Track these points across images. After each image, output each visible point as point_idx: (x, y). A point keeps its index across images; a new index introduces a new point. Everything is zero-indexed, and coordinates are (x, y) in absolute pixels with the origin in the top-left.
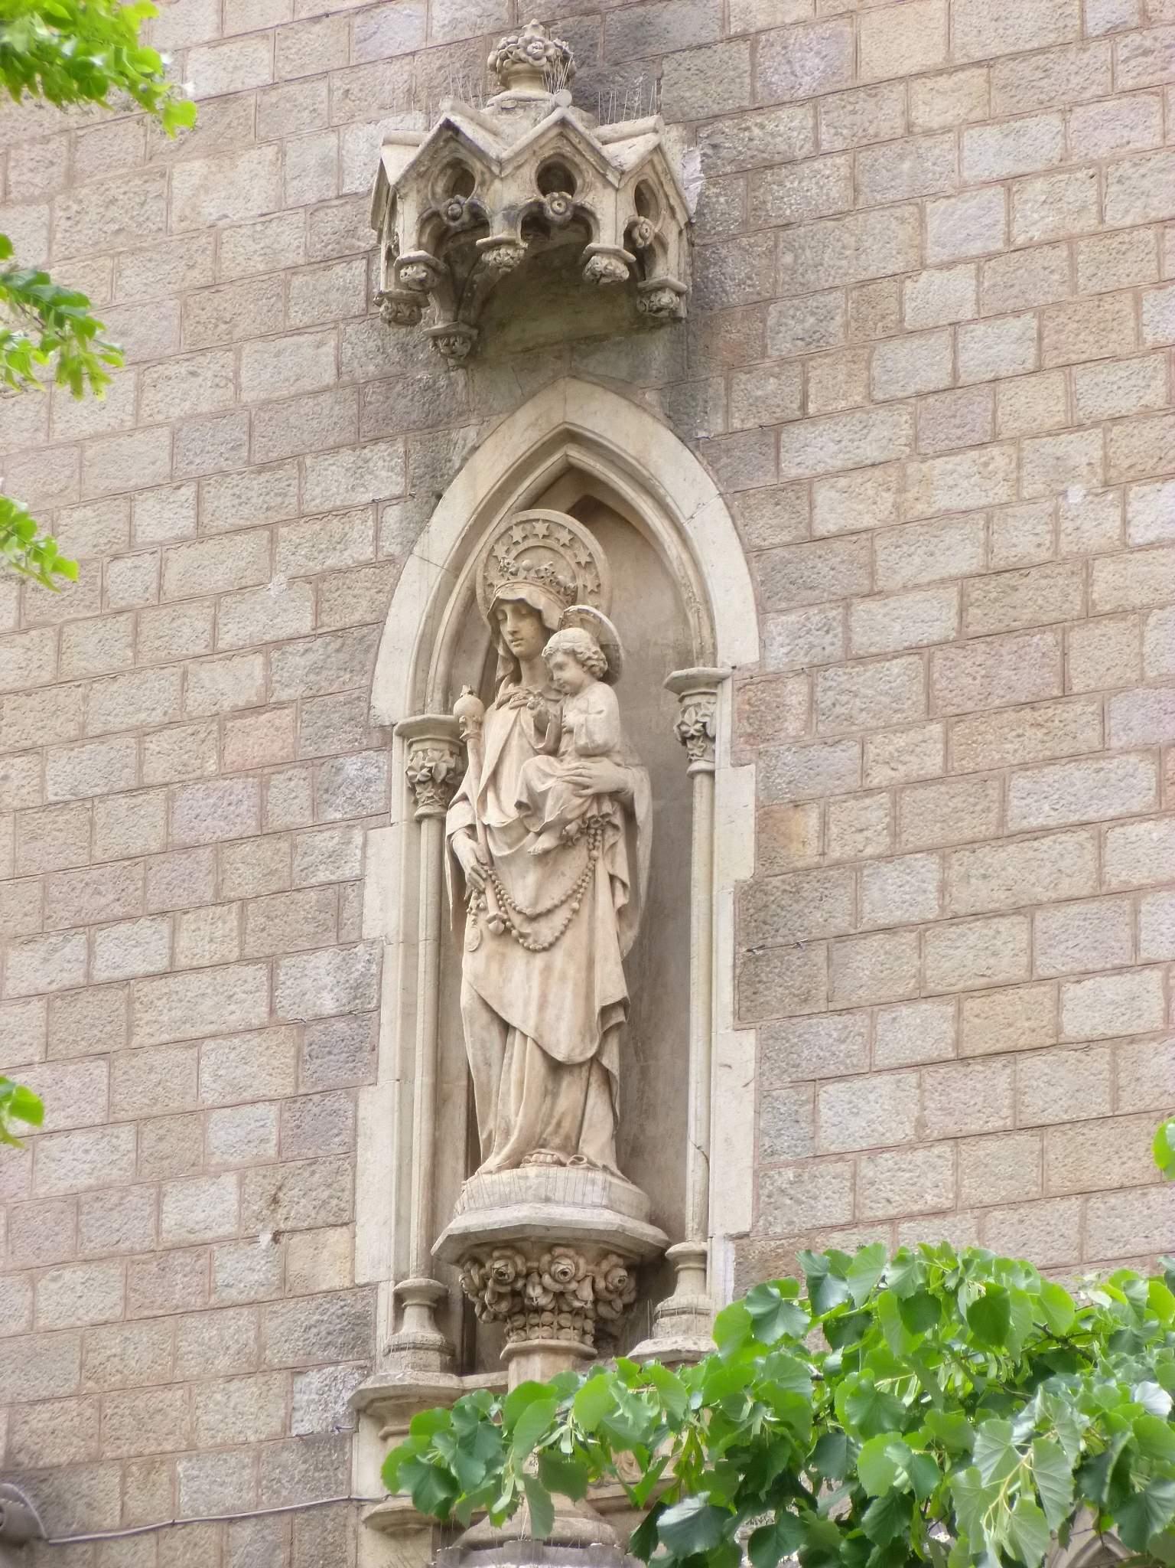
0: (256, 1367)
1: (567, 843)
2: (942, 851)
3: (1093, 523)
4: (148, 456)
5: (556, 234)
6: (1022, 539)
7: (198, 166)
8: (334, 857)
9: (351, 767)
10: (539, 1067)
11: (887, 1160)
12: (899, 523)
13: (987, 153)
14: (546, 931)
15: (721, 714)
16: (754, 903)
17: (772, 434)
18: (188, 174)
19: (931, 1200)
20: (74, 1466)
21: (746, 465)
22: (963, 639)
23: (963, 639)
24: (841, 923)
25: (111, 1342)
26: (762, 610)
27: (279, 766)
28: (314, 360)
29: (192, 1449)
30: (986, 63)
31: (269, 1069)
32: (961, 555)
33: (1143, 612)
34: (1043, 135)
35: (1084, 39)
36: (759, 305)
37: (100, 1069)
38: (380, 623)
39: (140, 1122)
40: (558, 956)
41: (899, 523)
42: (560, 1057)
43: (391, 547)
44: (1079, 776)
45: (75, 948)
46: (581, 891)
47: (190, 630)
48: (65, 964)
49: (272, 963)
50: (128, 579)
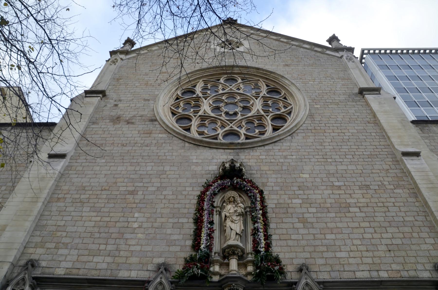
2: (276, 223)
4: (188, 184)
6: (281, 201)
7: (194, 167)
10: (235, 233)
14: (236, 222)
18: (193, 167)
20: (173, 264)
23: (276, 208)
25: (179, 253)
30: (273, 170)
32: (276, 202)
33: (295, 208)
35: (282, 170)
37: (179, 230)
39: (183, 235)
40: (238, 224)
42: (238, 232)
44: (290, 219)
46: (240, 219)
48: (176, 220)
50: (184, 193)
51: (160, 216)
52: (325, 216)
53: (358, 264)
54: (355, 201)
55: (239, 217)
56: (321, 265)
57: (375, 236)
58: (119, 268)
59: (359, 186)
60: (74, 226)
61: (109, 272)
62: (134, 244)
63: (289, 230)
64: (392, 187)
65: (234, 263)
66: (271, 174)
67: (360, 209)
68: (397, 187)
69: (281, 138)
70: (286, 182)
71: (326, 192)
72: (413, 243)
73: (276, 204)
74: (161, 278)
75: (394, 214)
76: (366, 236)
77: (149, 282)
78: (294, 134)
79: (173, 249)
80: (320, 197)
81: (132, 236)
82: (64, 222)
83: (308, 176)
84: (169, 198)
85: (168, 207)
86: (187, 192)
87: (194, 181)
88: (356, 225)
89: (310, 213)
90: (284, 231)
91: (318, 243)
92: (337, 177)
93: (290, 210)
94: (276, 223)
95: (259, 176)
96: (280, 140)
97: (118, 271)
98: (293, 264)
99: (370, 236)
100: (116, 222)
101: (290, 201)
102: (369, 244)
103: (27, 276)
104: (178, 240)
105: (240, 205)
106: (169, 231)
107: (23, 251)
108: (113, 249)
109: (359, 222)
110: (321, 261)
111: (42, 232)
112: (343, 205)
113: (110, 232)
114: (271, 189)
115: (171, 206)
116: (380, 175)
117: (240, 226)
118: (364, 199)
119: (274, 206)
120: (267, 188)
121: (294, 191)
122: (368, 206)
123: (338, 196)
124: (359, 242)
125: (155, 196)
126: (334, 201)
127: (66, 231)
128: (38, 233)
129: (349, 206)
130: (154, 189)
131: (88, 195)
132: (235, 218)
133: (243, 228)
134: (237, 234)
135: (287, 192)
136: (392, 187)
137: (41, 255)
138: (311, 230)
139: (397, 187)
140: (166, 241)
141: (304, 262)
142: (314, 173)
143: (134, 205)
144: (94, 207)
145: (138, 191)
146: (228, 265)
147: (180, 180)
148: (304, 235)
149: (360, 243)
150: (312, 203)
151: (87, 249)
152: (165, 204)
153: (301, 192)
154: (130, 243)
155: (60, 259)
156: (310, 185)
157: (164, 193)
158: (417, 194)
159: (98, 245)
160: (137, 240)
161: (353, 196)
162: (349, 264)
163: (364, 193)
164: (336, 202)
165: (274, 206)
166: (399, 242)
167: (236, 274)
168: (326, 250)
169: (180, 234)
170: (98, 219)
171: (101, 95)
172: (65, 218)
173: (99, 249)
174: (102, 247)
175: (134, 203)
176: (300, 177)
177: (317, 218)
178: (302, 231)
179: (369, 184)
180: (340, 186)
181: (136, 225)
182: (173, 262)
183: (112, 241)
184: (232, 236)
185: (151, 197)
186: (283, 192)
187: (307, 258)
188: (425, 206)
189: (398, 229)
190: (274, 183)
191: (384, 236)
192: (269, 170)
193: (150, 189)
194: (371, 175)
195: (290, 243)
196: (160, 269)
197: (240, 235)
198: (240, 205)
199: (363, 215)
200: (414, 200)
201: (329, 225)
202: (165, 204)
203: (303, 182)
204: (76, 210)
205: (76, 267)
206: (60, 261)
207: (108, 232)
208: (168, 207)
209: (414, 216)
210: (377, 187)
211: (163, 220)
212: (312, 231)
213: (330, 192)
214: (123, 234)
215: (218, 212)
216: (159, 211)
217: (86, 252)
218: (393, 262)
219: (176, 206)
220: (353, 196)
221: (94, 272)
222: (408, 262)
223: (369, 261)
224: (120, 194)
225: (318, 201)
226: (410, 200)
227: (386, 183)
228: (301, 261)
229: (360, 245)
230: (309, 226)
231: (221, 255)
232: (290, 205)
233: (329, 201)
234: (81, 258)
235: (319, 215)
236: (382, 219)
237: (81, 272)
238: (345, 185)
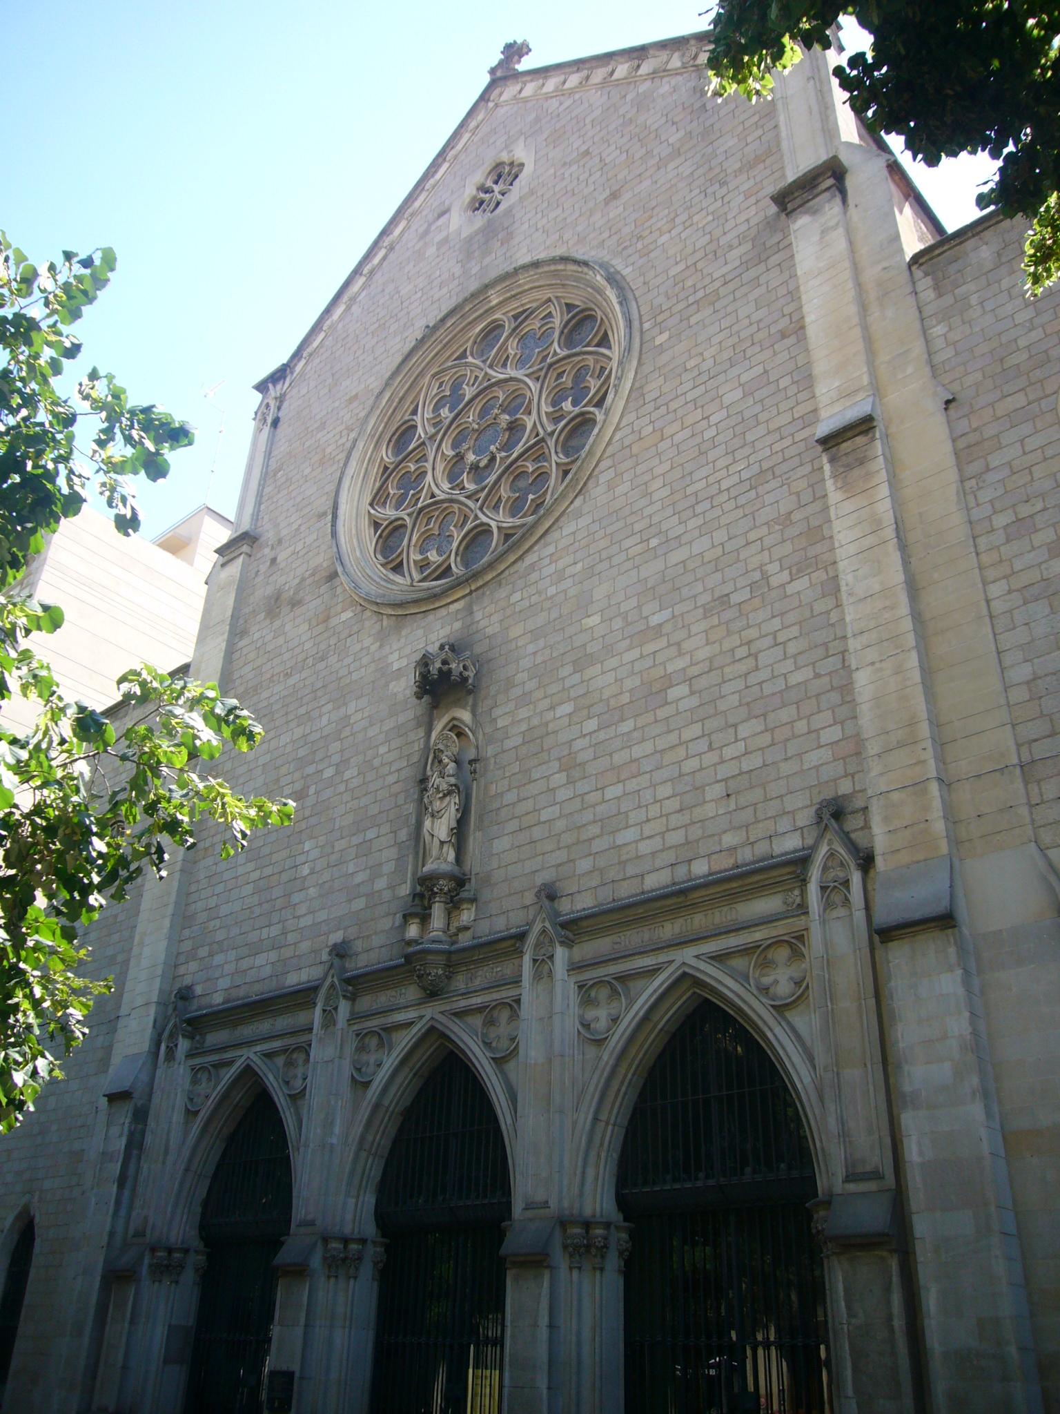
1: (445, 796)
2: (518, 787)
3: (549, 716)
5: (445, 675)
13: (531, 648)
22: (523, 744)
28: (410, 714)
29: (376, 933)
32: (524, 727)
34: (541, 643)
36: (488, 687)
41: (513, 723)
44: (544, 767)
68: (799, 571)
69: (557, 514)
77: (315, 989)
78: (591, 484)
88: (673, 738)
91: (588, 816)
96: (557, 520)
99: (692, 764)
110: (584, 865)
128: (186, 933)
139: (799, 571)
161: (686, 646)
163: (712, 627)
164: (642, 684)
166: (755, 761)
171: (245, 548)
180: (660, 625)
187: (560, 865)
195: (537, 833)
199: (694, 701)
212: (582, 787)
213: (635, 653)
227: (773, 568)
229: (668, 798)
235: (602, 735)
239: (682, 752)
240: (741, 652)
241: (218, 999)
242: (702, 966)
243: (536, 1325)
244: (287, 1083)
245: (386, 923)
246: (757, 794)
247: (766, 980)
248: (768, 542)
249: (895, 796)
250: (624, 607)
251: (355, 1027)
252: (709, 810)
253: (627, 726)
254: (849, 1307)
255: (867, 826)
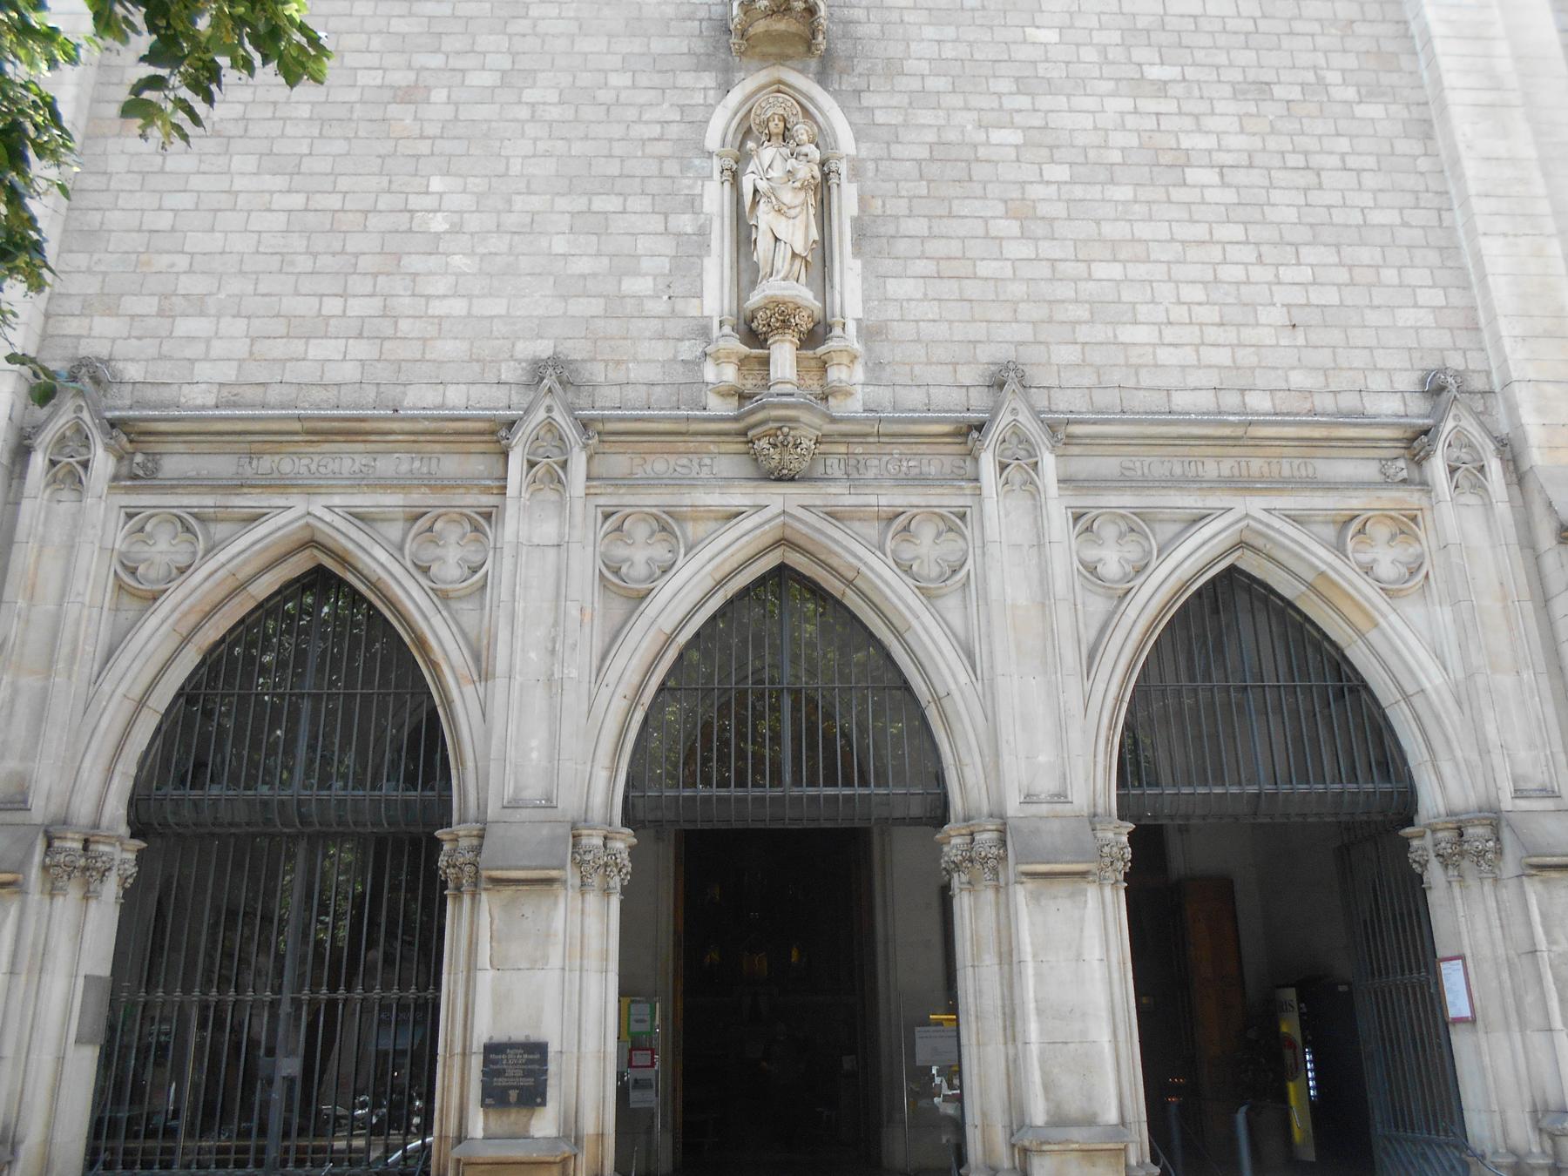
0: (661, 337)
2: (930, 218)
6: (952, 136)
8: (690, 187)
9: (697, 162)
11: (913, 304)
12: (906, 125)
14: (792, 213)
15: (843, 168)
16: (857, 223)
17: (858, 93)
19: (930, 316)
20: (583, 361)
21: (850, 100)
23: (932, 159)
24: (892, 231)
25: (601, 323)
26: (857, 140)
27: (667, 157)
29: (635, 360)
31: (667, 246)
32: (930, 136)
33: (997, 163)
34: (950, 32)
36: (851, 58)
37: (594, 238)
38: (707, 122)
39: (611, 256)
40: (797, 221)
41: (906, 125)
43: (710, 101)
44: (977, 203)
45: (584, 200)
47: (632, 114)
48: (580, 203)
49: (666, 216)
51: (522, 186)
52: (1098, 196)
53: (1183, 367)
54: (1209, 142)
55: (802, 194)
56: (1066, 366)
57: (1258, 273)
58: (403, 378)
59: (1233, 84)
60: (213, 230)
61: (370, 394)
62: (441, 292)
63: (973, 242)
64: (1351, 94)
65: (784, 356)
66: (920, 25)
67: (1222, 175)
70: (972, 60)
71: (1113, 104)
72: (1376, 303)
73: (931, 145)
74: (549, 409)
75: (1334, 198)
76: (1227, 273)
79: (580, 307)
80: (1086, 121)
81: (433, 262)
82: (171, 214)
83: (1051, 36)
84: (548, 117)
85: (547, 155)
86: (613, 94)
87: (637, 46)
88: (1200, 231)
89: (1048, 183)
90: (954, 248)
91: (1064, 291)
92: (1160, 47)
93: (980, 171)
94: (930, 218)
95: (874, 29)
97: (401, 388)
98: (978, 363)
99: (1237, 273)
100: (366, 212)
101: (980, 136)
102: (1231, 300)
103: (86, 415)
104: (595, 275)
105: (804, 149)
106: (560, 245)
107: (44, 329)
108: (372, 313)
109: (1210, 223)
110: (1065, 355)
111: (96, 257)
112: (1166, 158)
113: (349, 249)
114: (915, 84)
115: (560, 146)
116: (1321, 41)
117: (807, 227)
118: (1243, 138)
119: (925, 154)
120: (904, 80)
121: (1000, 95)
122: (1251, 166)
123: (1150, 123)
124: (1197, 294)
125: (496, 107)
126: (1135, 142)
127: (186, 249)
129: (1184, 161)
130: (488, 79)
131: (240, 108)
132: (788, 197)
133: (814, 234)
134: (794, 255)
135: (975, 101)
136: (1351, 94)
137: (114, 340)
138: (1044, 245)
140: (551, 279)
141: (1012, 355)
142: (1077, 24)
143: (424, 147)
144: (271, 153)
145: (428, 89)
146: (765, 362)
147: (584, 45)
148: (1018, 264)
149: (1203, 298)
150: (1058, 147)
151: (278, 316)
152: (535, 140)
153: (1024, 102)
154: (430, 291)
155: (188, 353)
156: (1056, 73)
157: (530, 95)
158: (1432, 126)
159: (317, 300)
160: (452, 279)
161: (1209, 123)
162: (1156, 366)
164: (1141, 147)
165: (925, 154)
166: (1330, 296)
167: (791, 395)
168: (1086, 315)
169: (598, 254)
170: (298, 201)
172: (172, 201)
173: (319, 315)
174: (332, 306)
175: (422, 137)
176: (1025, 41)
177: (1068, 201)
178: (1016, 250)
179: (1269, 76)
180: (1165, 83)
181: (439, 223)
182: (585, 355)
183: (359, 285)
184: (778, 264)
185: (482, 111)
186: (957, 101)
187: (1022, 343)
188: (1447, 174)
189: (1339, 252)
190: (930, 60)
191: (1287, 274)
192: (915, 8)
193: (475, 79)
194: (1286, 42)
195: (972, 289)
196: (542, 379)
197: (805, 258)
198: (804, 149)
199: (1230, 196)
200: (1416, 147)
201: (1107, 229)
202: (535, 140)
203: (1034, 62)
204: (204, 167)
205: (253, 380)
206: (192, 361)
207: (343, 252)
208: (547, 155)
209: (1401, 209)
210: (1295, 93)
211: (536, 202)
212: (1048, 249)
214: (398, 257)
215: (727, 173)
216: (516, 167)
217: (279, 327)
218: (1296, 363)
219: (577, 148)
220: (1209, 123)
221: (318, 395)
222: (1346, 365)
223: (1222, 357)
224: (362, 102)
225: (1081, 140)
226: (1402, 146)
227: (1333, 77)
228: (1004, 353)
229: (1200, 304)
230: (1039, 229)
231: (743, 327)
232: (982, 152)
233: (1118, 139)
234: (262, 347)
235: (1078, 191)
236: (1291, 215)
237: (273, 395)
238: (1184, 79)
239: (1216, 253)
240: (1295, 160)
241: (199, 397)
242: (1277, 523)
243: (1079, 958)
244: (425, 571)
245: (661, 351)
246: (1336, 336)
247: (1364, 558)
248: (1321, 41)
249: (1549, 389)
250: (1098, 37)
251: (602, 501)
252: (1266, 336)
253: (1123, 193)
254: (1547, 933)
255: (1512, 409)
